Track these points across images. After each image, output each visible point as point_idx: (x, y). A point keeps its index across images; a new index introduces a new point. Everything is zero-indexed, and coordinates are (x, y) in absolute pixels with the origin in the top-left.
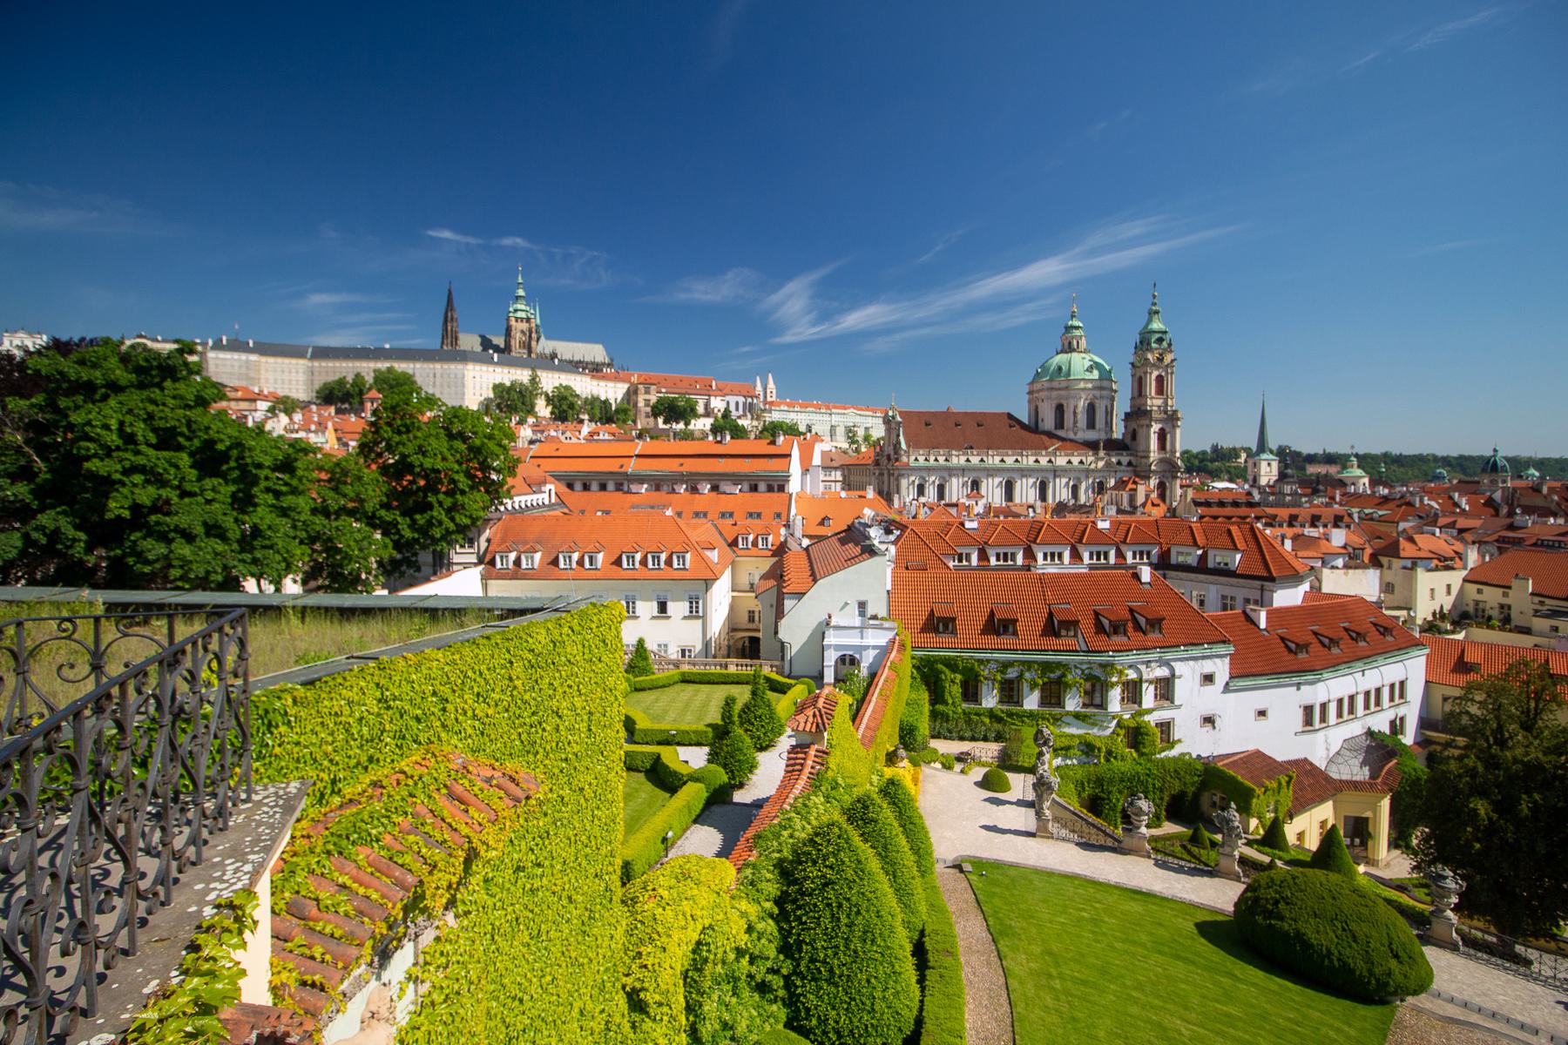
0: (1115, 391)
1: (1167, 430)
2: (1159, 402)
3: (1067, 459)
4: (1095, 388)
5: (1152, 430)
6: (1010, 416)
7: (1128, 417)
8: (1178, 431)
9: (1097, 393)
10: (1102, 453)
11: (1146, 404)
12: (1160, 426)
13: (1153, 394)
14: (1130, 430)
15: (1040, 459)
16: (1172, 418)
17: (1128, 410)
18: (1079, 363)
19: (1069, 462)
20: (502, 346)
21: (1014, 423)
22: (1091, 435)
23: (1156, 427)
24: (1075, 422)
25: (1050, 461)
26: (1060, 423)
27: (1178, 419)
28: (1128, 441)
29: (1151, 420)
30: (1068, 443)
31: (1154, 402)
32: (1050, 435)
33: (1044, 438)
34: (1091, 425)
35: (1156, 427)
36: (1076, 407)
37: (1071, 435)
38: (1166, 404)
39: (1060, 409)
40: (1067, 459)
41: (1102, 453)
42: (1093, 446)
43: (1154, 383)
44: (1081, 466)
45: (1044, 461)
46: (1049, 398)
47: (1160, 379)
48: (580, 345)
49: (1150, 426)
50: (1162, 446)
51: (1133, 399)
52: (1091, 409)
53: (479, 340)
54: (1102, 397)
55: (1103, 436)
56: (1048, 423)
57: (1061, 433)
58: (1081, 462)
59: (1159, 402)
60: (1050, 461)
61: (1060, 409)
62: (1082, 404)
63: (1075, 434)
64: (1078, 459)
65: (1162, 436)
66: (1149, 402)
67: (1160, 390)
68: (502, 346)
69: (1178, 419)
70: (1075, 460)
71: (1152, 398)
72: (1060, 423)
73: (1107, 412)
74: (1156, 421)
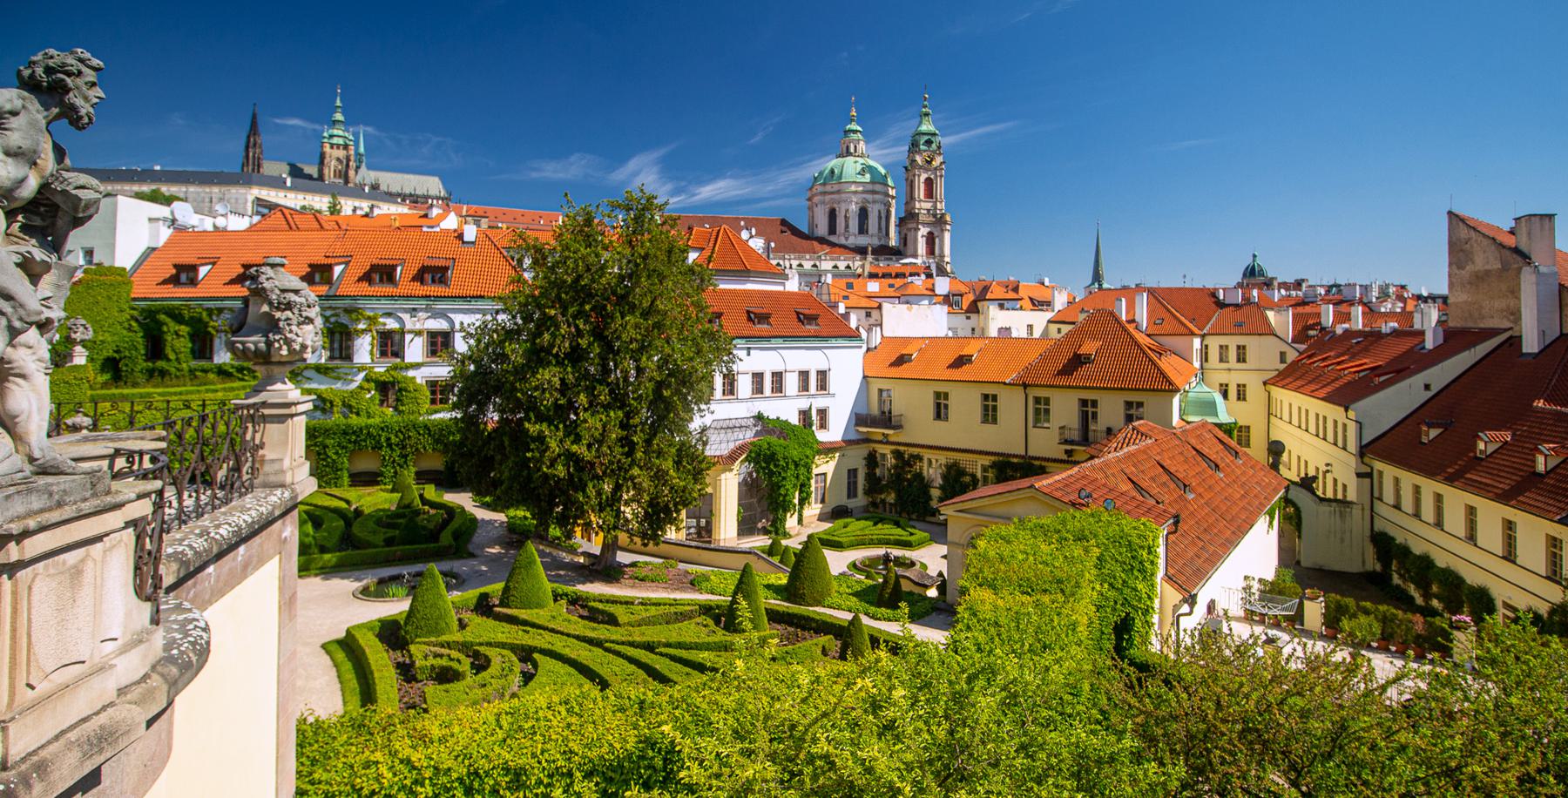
0: (893, 197)
1: (936, 234)
2: (929, 205)
3: (833, 263)
4: (864, 192)
5: (920, 234)
6: (784, 222)
7: (902, 222)
8: (947, 236)
9: (869, 197)
10: (870, 258)
11: (914, 208)
12: (928, 230)
13: (922, 197)
14: (903, 236)
15: (803, 263)
16: (939, 221)
17: (903, 215)
18: (850, 167)
19: (835, 267)
20: (316, 176)
21: (784, 229)
22: (862, 241)
23: (923, 231)
24: (847, 226)
25: (815, 266)
26: (832, 230)
27: (946, 223)
28: (902, 248)
29: (918, 223)
30: (837, 249)
31: (922, 206)
32: (822, 241)
33: (815, 243)
34: (863, 230)
35: (923, 231)
36: (847, 211)
37: (843, 241)
38: (936, 208)
39: (832, 215)
40: (832, 263)
41: (870, 258)
42: (861, 251)
43: (922, 186)
44: (849, 271)
45: (808, 265)
46: (823, 203)
47: (929, 182)
48: (411, 177)
49: (917, 229)
50: (931, 251)
51: (907, 203)
52: (863, 214)
53: (288, 168)
54: (874, 202)
55: (876, 242)
56: (822, 230)
57: (833, 239)
58: (848, 267)
59: (929, 205)
60: (815, 266)
61: (832, 215)
62: (854, 208)
63: (847, 239)
64: (846, 263)
65: (931, 239)
66: (917, 205)
67: (930, 194)
68: (316, 176)
69: (946, 223)
70: (842, 265)
71: (920, 201)
72: (832, 230)
73: (880, 218)
74: (924, 224)
